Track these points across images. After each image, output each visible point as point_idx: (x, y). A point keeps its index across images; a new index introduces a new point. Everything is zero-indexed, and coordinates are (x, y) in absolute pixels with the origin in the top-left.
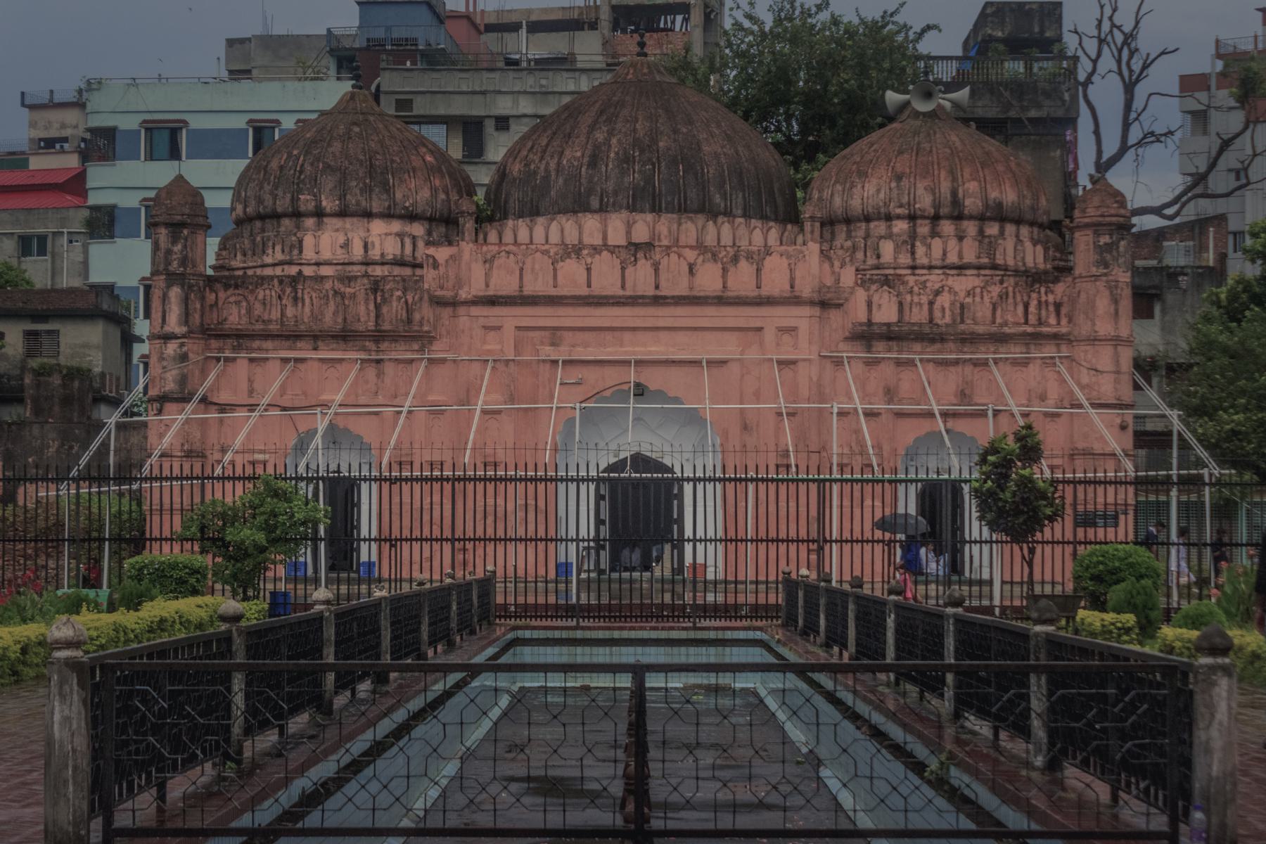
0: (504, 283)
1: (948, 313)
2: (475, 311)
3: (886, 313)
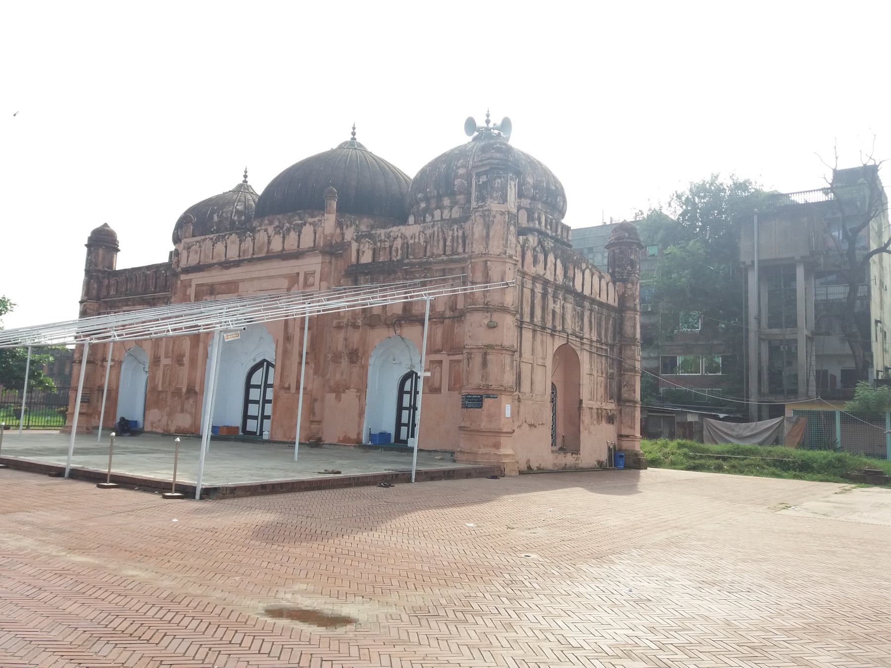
0: (194, 260)
1: (400, 252)
2: (183, 277)
3: (366, 258)
